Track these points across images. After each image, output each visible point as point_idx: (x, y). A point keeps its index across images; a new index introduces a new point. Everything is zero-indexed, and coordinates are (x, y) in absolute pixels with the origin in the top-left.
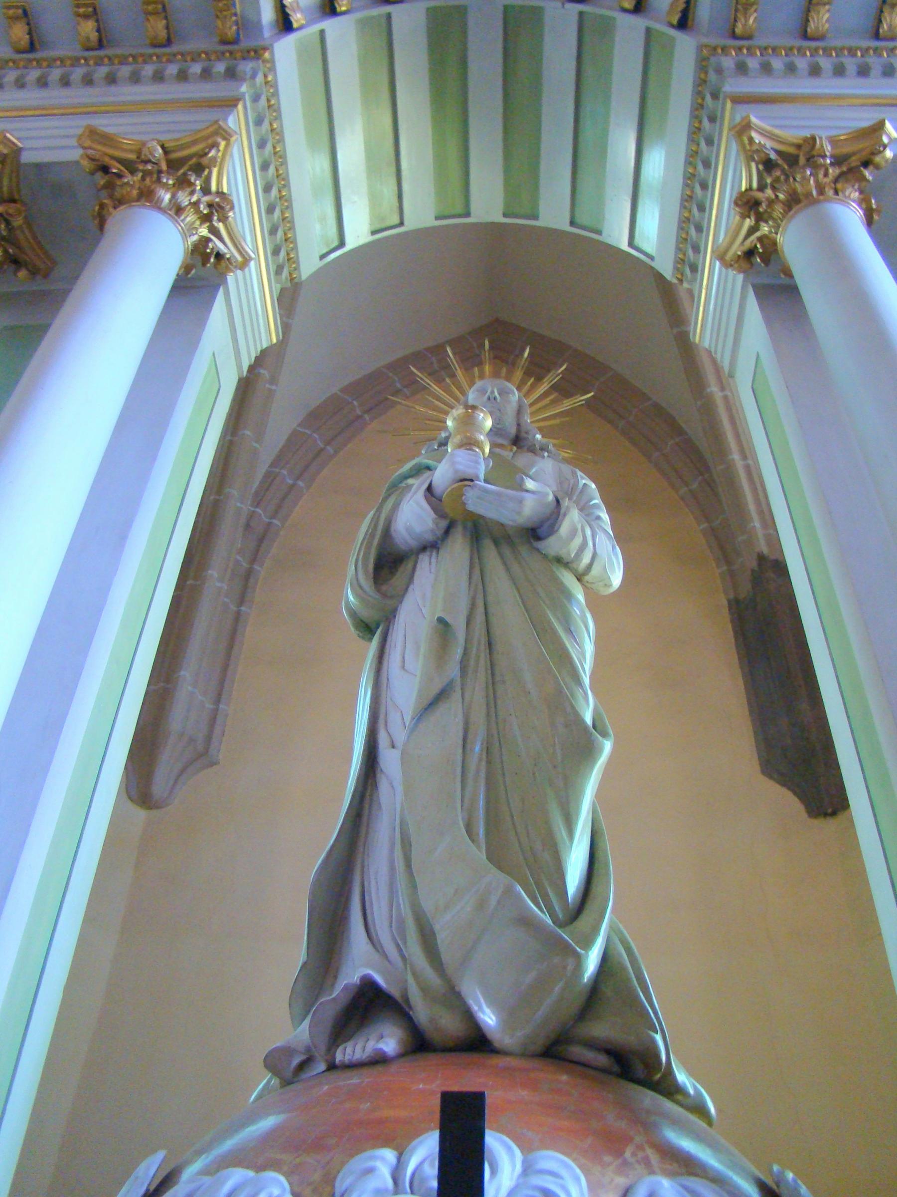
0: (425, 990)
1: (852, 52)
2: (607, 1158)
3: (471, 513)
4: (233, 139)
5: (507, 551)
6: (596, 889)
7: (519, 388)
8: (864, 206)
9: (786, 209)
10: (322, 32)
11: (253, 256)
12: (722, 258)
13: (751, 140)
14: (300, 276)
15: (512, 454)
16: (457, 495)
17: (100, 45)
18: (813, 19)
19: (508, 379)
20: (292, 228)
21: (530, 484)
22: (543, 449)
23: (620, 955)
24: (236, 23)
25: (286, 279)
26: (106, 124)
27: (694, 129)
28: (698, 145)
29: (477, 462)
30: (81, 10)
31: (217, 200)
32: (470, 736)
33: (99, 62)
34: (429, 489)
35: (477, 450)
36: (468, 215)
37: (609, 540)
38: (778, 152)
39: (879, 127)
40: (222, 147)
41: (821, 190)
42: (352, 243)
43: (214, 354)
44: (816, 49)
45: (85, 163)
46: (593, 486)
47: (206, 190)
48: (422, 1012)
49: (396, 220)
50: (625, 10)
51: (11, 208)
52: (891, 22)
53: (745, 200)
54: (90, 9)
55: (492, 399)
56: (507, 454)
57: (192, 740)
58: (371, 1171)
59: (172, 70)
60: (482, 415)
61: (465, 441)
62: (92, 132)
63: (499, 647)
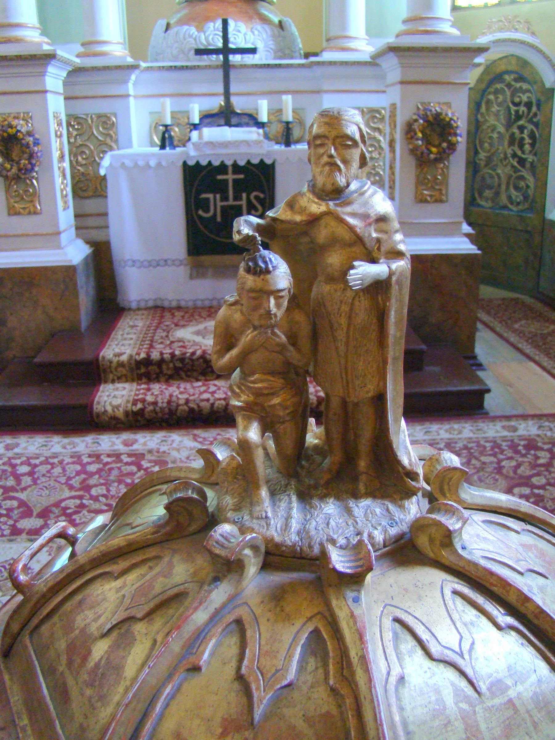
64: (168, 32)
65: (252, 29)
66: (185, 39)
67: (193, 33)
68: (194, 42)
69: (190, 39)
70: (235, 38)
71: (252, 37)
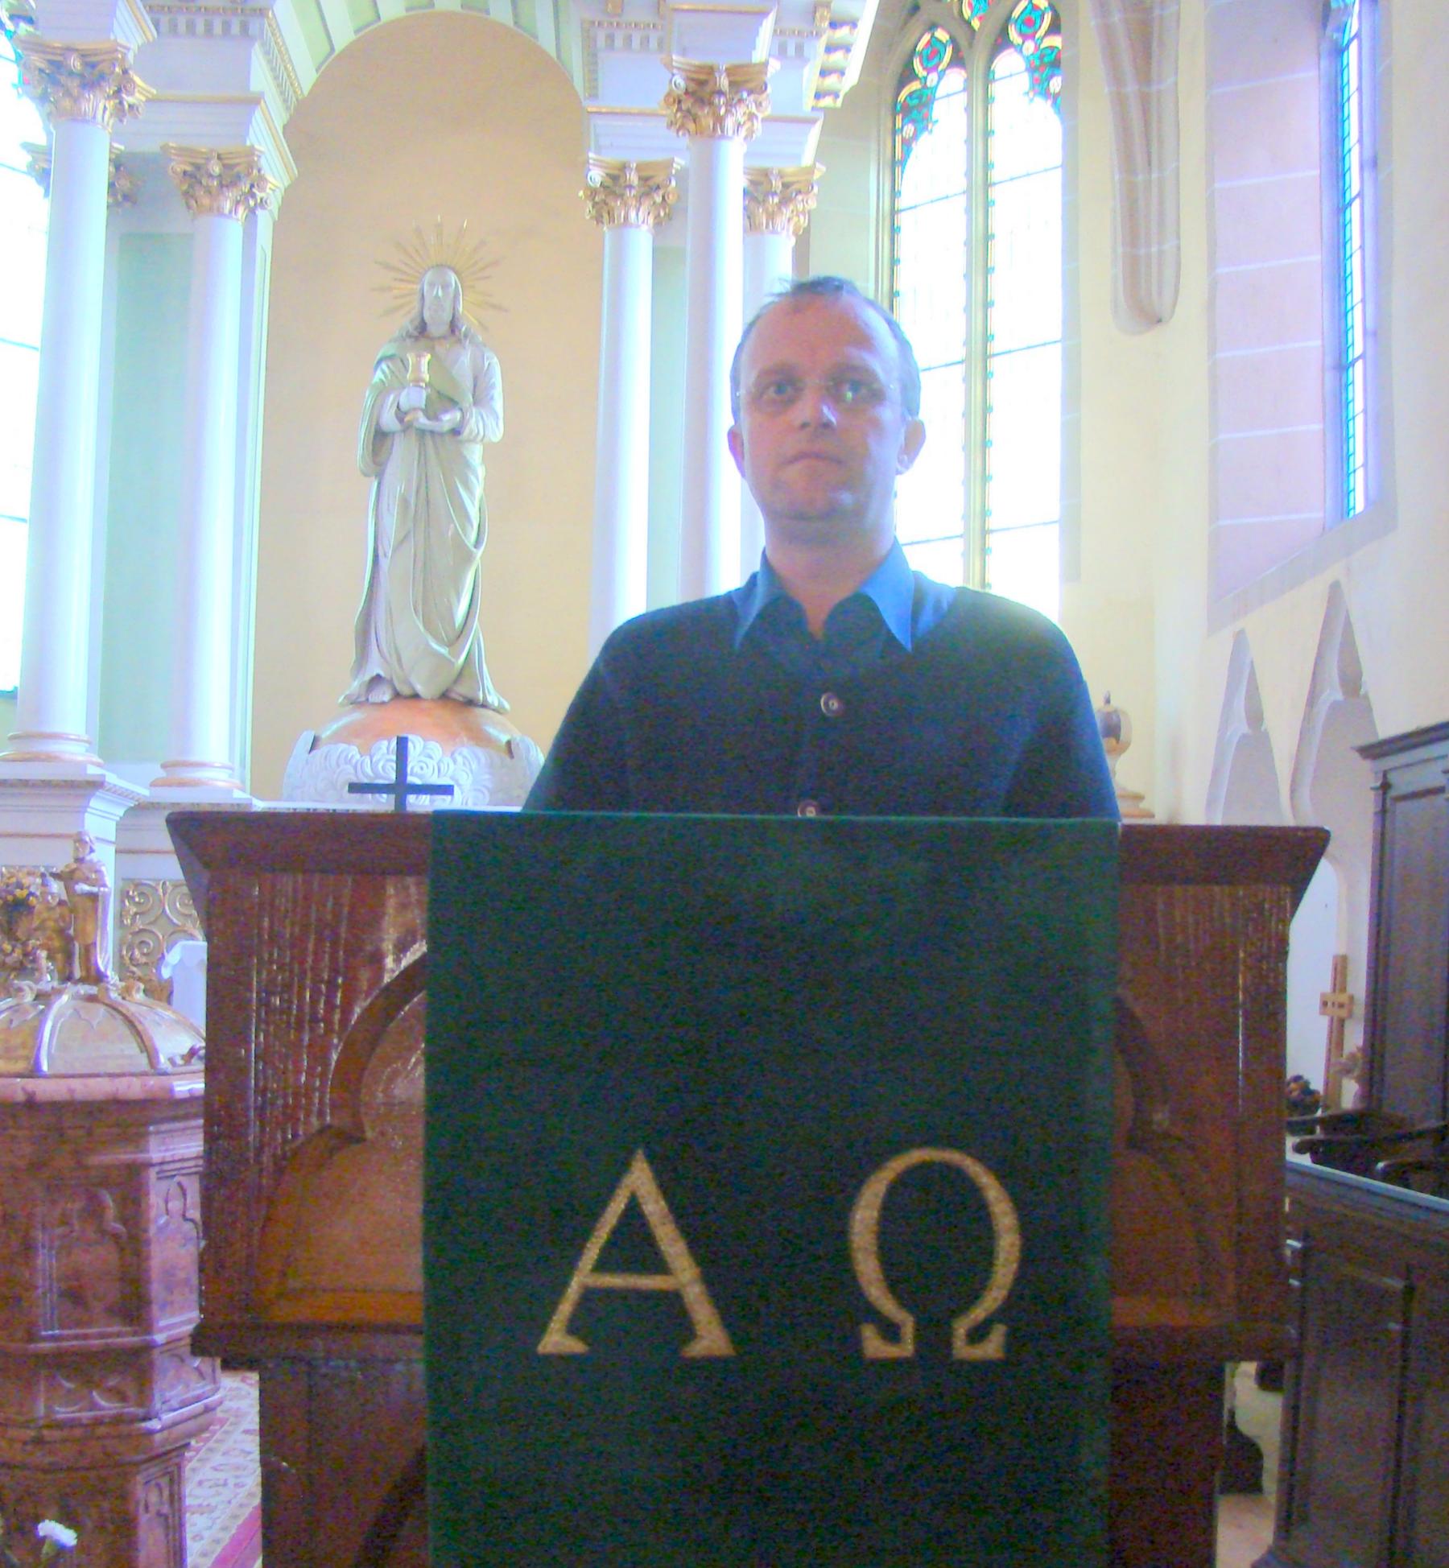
22: (466, 336)
39: (672, 161)
42: (338, 49)
48: (399, 687)
58: (380, 748)
64: (314, 752)
65: (452, 754)
66: (338, 765)
68: (352, 771)
69: (349, 766)
70: (422, 768)
71: (452, 766)
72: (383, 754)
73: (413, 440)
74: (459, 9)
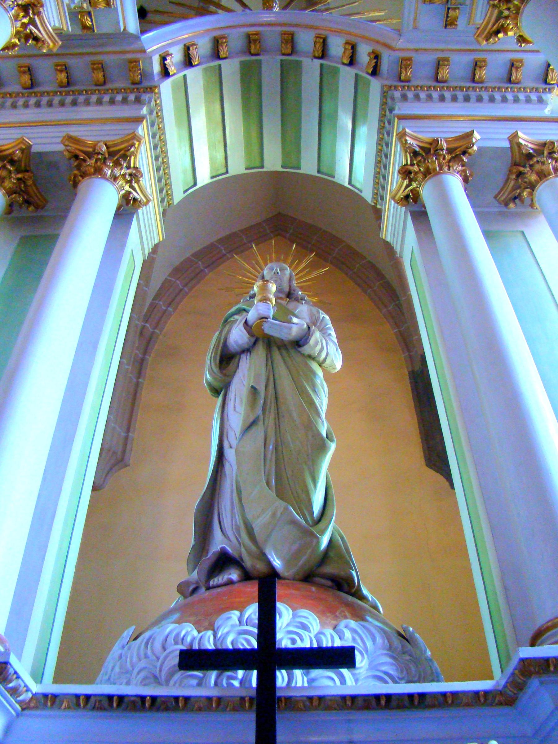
0: (249, 553)
1: (461, 89)
2: (328, 614)
3: (266, 334)
4: (142, 141)
5: (284, 352)
6: (328, 512)
7: (290, 267)
8: (463, 174)
9: (424, 176)
10: (185, 77)
11: (151, 198)
12: (393, 198)
13: (406, 140)
14: (174, 203)
15: (286, 302)
16: (260, 326)
17: (68, 84)
18: (440, 72)
19: (285, 261)
20: (169, 178)
21: (295, 320)
22: (302, 299)
23: (338, 540)
24: (140, 74)
25: (166, 204)
26: (76, 132)
27: (381, 127)
28: (383, 135)
29: (269, 309)
30: (59, 68)
31: (134, 172)
32: (267, 442)
33: (68, 93)
34: (246, 322)
35: (269, 303)
36: (263, 167)
37: (335, 345)
38: (419, 146)
39: (472, 133)
40: (136, 146)
41: (441, 169)
42: (200, 184)
43: (132, 250)
44: (443, 87)
45: (66, 153)
46: (327, 317)
47: (128, 167)
48: (248, 562)
49: (224, 171)
50: (344, 64)
51: (27, 175)
52: (480, 75)
53: (404, 171)
54: (64, 67)
55: (276, 273)
56: (284, 302)
57: (114, 453)
59: (106, 98)
60: (271, 284)
61: (263, 298)
62: (70, 138)
63: (281, 400)
66: (164, 649)
67: (187, 633)
72: (233, 626)
73: (260, 352)
74: (280, 169)
